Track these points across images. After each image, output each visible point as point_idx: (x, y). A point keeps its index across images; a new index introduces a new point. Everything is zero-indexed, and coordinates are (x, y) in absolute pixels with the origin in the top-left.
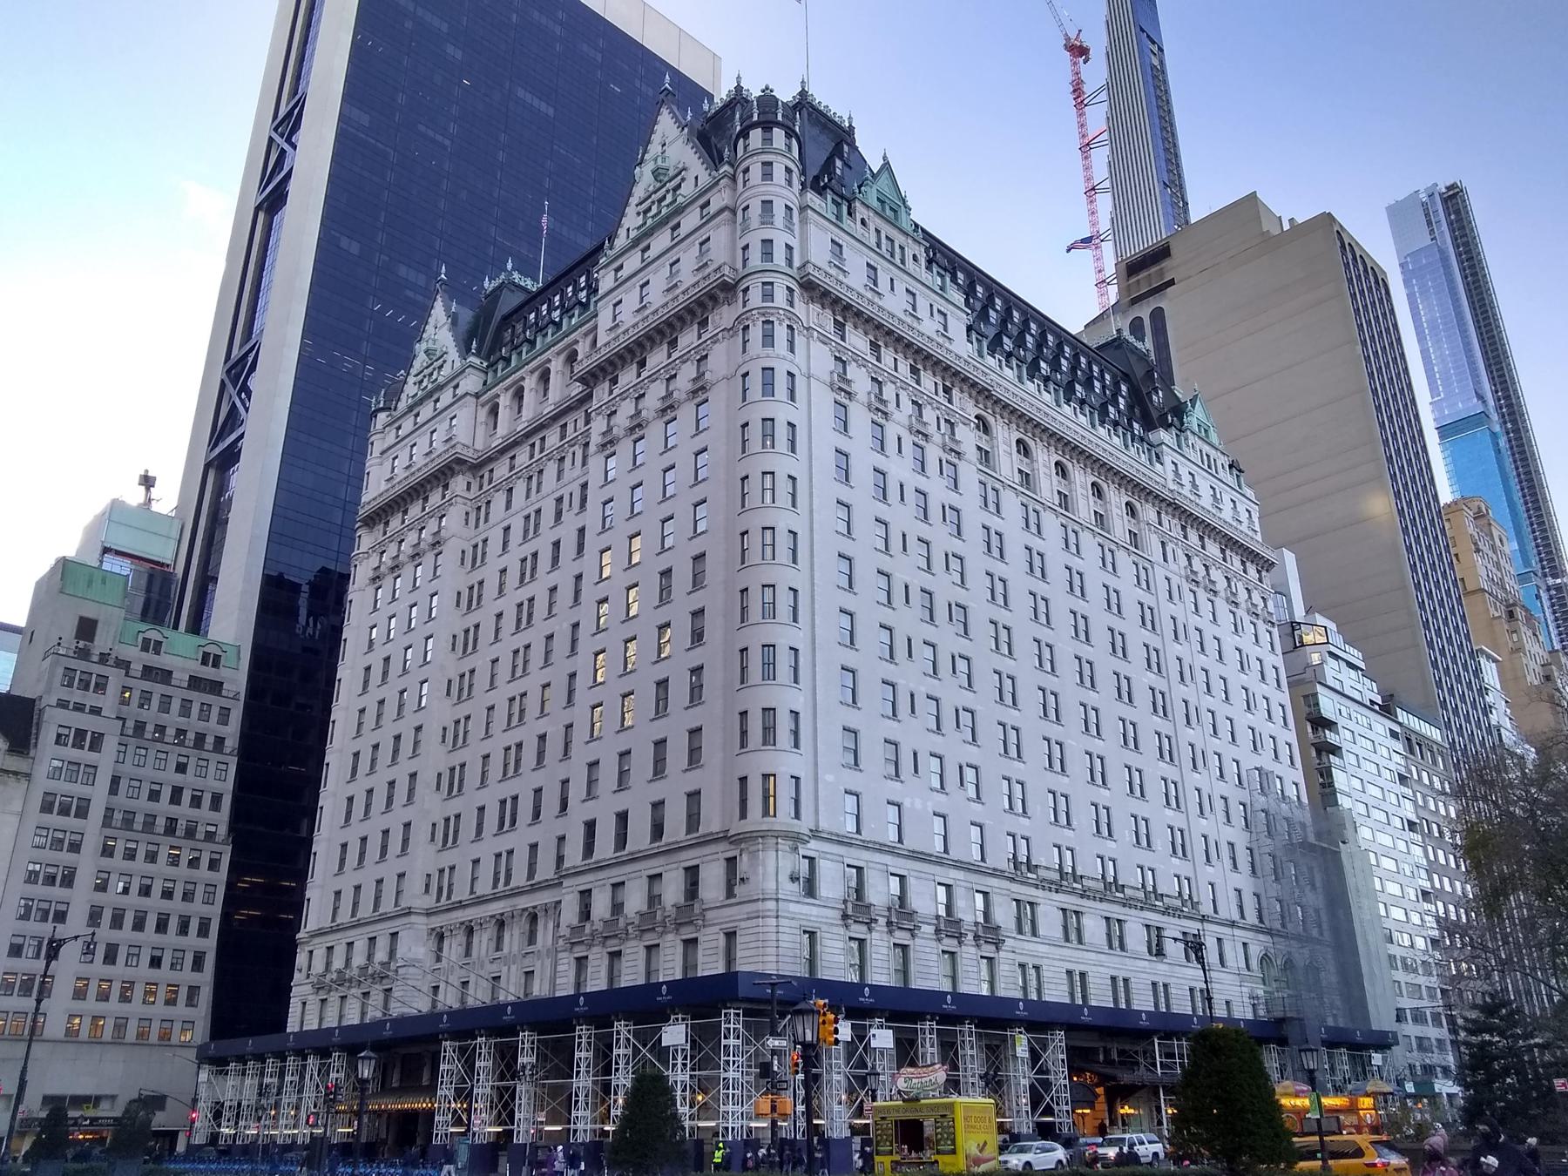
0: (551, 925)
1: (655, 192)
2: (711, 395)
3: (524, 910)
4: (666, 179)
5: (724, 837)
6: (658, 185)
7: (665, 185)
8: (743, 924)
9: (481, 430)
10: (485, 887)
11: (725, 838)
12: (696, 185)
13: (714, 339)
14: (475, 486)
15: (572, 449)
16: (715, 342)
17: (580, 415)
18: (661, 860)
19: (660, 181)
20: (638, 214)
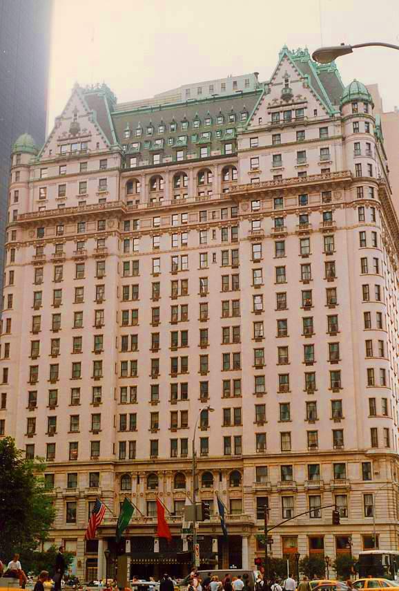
0: (225, 480)
1: (283, 106)
2: (336, 234)
3: (200, 470)
4: (290, 102)
5: (363, 453)
6: (284, 103)
7: (291, 105)
8: (376, 492)
9: (123, 192)
10: (164, 453)
11: (363, 454)
12: (316, 114)
13: (338, 206)
14: (122, 226)
15: (212, 229)
16: (337, 207)
17: (218, 209)
18: (318, 459)
19: (287, 101)
20: (269, 113)
